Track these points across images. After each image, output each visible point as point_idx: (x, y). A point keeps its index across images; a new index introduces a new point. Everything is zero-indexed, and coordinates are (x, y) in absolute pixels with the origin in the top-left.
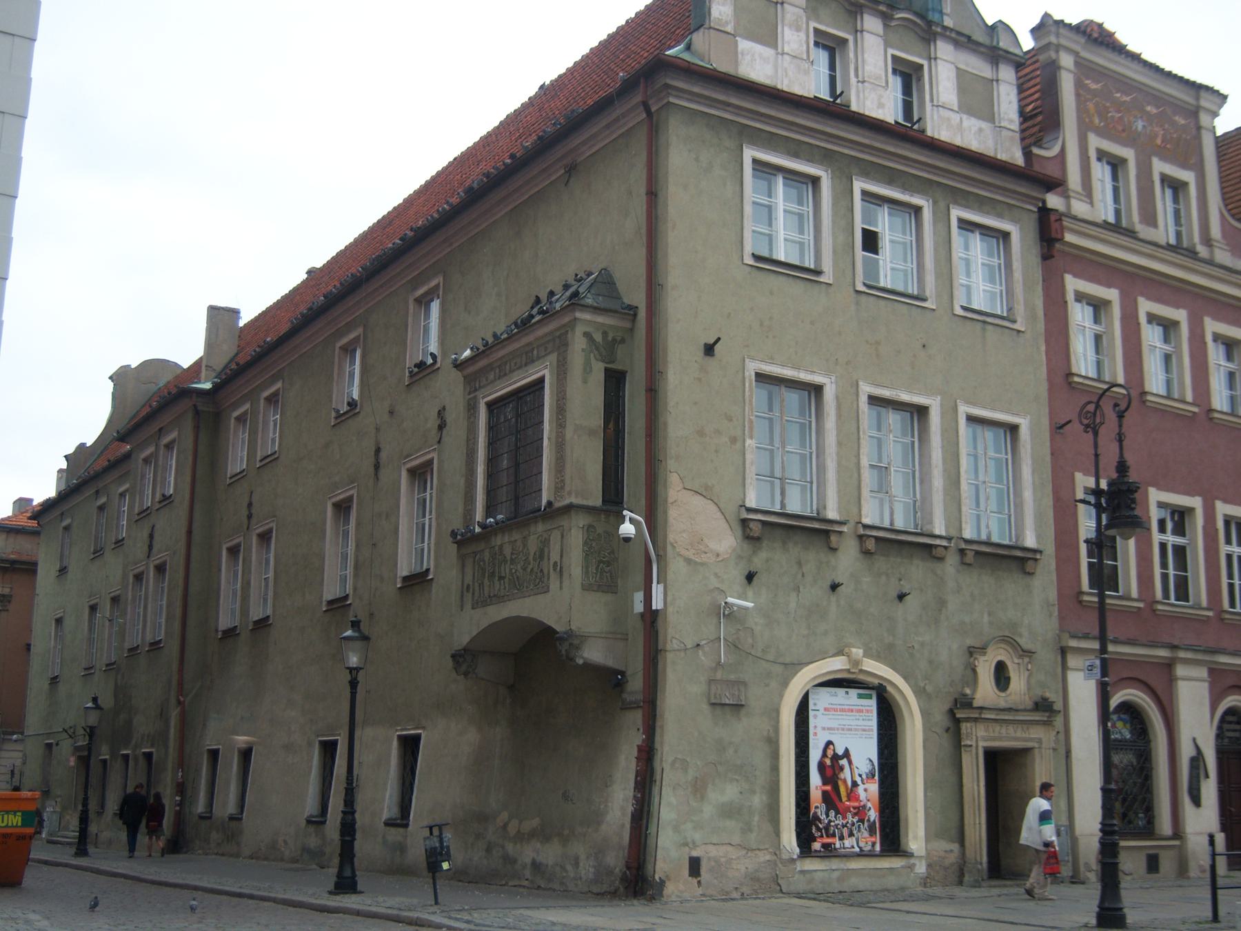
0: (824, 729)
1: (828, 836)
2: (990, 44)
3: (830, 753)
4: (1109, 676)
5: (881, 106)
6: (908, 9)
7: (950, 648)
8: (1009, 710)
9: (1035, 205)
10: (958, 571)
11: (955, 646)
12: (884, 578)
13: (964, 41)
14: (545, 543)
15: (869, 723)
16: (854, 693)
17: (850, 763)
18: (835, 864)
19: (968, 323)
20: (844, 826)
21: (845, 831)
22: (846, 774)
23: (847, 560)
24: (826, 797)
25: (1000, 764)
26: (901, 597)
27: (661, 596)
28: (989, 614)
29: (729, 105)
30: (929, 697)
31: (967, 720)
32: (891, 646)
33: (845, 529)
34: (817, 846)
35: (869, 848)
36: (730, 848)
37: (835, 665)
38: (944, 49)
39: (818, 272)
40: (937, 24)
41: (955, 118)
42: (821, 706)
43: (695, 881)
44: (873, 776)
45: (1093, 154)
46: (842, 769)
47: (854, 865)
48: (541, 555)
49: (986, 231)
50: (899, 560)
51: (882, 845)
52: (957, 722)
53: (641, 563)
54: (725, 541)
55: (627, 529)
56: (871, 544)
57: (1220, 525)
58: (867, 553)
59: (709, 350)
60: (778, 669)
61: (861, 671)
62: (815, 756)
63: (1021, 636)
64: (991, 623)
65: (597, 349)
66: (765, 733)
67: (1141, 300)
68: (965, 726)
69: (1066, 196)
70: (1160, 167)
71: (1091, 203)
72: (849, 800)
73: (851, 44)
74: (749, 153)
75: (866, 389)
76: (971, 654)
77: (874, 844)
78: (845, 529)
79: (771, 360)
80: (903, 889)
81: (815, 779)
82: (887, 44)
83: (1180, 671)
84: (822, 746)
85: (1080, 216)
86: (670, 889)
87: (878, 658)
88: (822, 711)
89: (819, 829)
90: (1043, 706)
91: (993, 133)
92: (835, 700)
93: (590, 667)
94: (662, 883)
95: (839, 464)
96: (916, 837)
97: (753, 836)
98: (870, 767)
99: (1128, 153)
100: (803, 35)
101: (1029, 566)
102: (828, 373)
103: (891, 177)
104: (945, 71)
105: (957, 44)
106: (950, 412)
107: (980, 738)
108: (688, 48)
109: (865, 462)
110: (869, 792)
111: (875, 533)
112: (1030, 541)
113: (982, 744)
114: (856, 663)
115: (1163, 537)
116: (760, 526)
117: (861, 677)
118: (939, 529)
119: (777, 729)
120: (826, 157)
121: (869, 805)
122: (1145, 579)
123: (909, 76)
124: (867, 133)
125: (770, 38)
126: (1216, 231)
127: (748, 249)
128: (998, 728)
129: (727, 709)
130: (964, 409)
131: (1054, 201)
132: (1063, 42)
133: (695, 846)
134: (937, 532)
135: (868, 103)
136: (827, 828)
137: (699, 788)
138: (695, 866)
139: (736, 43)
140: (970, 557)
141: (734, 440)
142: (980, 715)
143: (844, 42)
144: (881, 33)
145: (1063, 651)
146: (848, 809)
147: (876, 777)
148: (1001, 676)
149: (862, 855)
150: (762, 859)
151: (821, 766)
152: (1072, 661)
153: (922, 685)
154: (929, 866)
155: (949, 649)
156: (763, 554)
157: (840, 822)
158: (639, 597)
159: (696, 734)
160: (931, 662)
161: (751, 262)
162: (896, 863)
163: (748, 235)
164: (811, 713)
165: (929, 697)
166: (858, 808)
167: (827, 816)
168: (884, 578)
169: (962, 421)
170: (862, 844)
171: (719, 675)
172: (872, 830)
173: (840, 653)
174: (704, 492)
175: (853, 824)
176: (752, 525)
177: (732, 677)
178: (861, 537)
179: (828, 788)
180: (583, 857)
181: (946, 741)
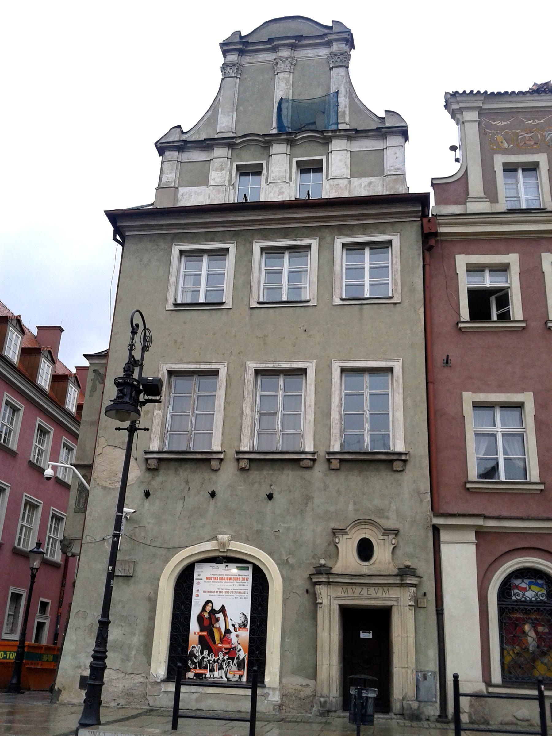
0: (205, 592)
1: (200, 668)
3: (208, 609)
7: (313, 531)
9: (417, 217)
10: (326, 475)
11: (319, 529)
12: (256, 486)
13: (354, 134)
15: (245, 587)
17: (225, 616)
19: (346, 307)
20: (215, 662)
21: (216, 666)
22: (221, 624)
23: (226, 477)
24: (202, 640)
26: (270, 497)
28: (355, 504)
29: (162, 225)
30: (292, 567)
31: (320, 583)
32: (259, 532)
34: (190, 675)
35: (236, 679)
37: (208, 547)
38: (337, 145)
42: (204, 576)
44: (245, 626)
45: (499, 169)
46: (217, 620)
47: (211, 690)
50: (271, 472)
51: (247, 679)
58: (242, 470)
60: (164, 552)
61: (228, 550)
62: (196, 610)
63: (388, 518)
64: (356, 510)
66: (147, 595)
72: (222, 642)
73: (265, 166)
76: (334, 534)
77: (241, 677)
79: (181, 362)
81: (194, 627)
84: (203, 603)
87: (247, 541)
88: (204, 579)
90: (405, 572)
97: (130, 664)
98: (243, 619)
101: (397, 465)
103: (285, 233)
105: (349, 138)
110: (241, 638)
111: (247, 456)
112: (399, 446)
114: (223, 545)
121: (240, 647)
124: (259, 213)
128: (358, 590)
129: (121, 579)
132: (462, 105)
134: (307, 450)
136: (200, 663)
140: (335, 464)
146: (220, 649)
147: (248, 627)
148: (365, 550)
149: (229, 685)
150: (136, 681)
151: (200, 618)
152: (444, 536)
153: (286, 559)
154: (284, 696)
155: (313, 532)
156: (160, 478)
159: (95, 595)
160: (295, 542)
161: (173, 308)
164: (195, 582)
165: (292, 567)
166: (230, 649)
167: (202, 653)
170: (228, 676)
172: (240, 665)
173: (214, 538)
175: (224, 661)
177: (127, 558)
178: (238, 460)
179: (205, 634)
181: (306, 600)
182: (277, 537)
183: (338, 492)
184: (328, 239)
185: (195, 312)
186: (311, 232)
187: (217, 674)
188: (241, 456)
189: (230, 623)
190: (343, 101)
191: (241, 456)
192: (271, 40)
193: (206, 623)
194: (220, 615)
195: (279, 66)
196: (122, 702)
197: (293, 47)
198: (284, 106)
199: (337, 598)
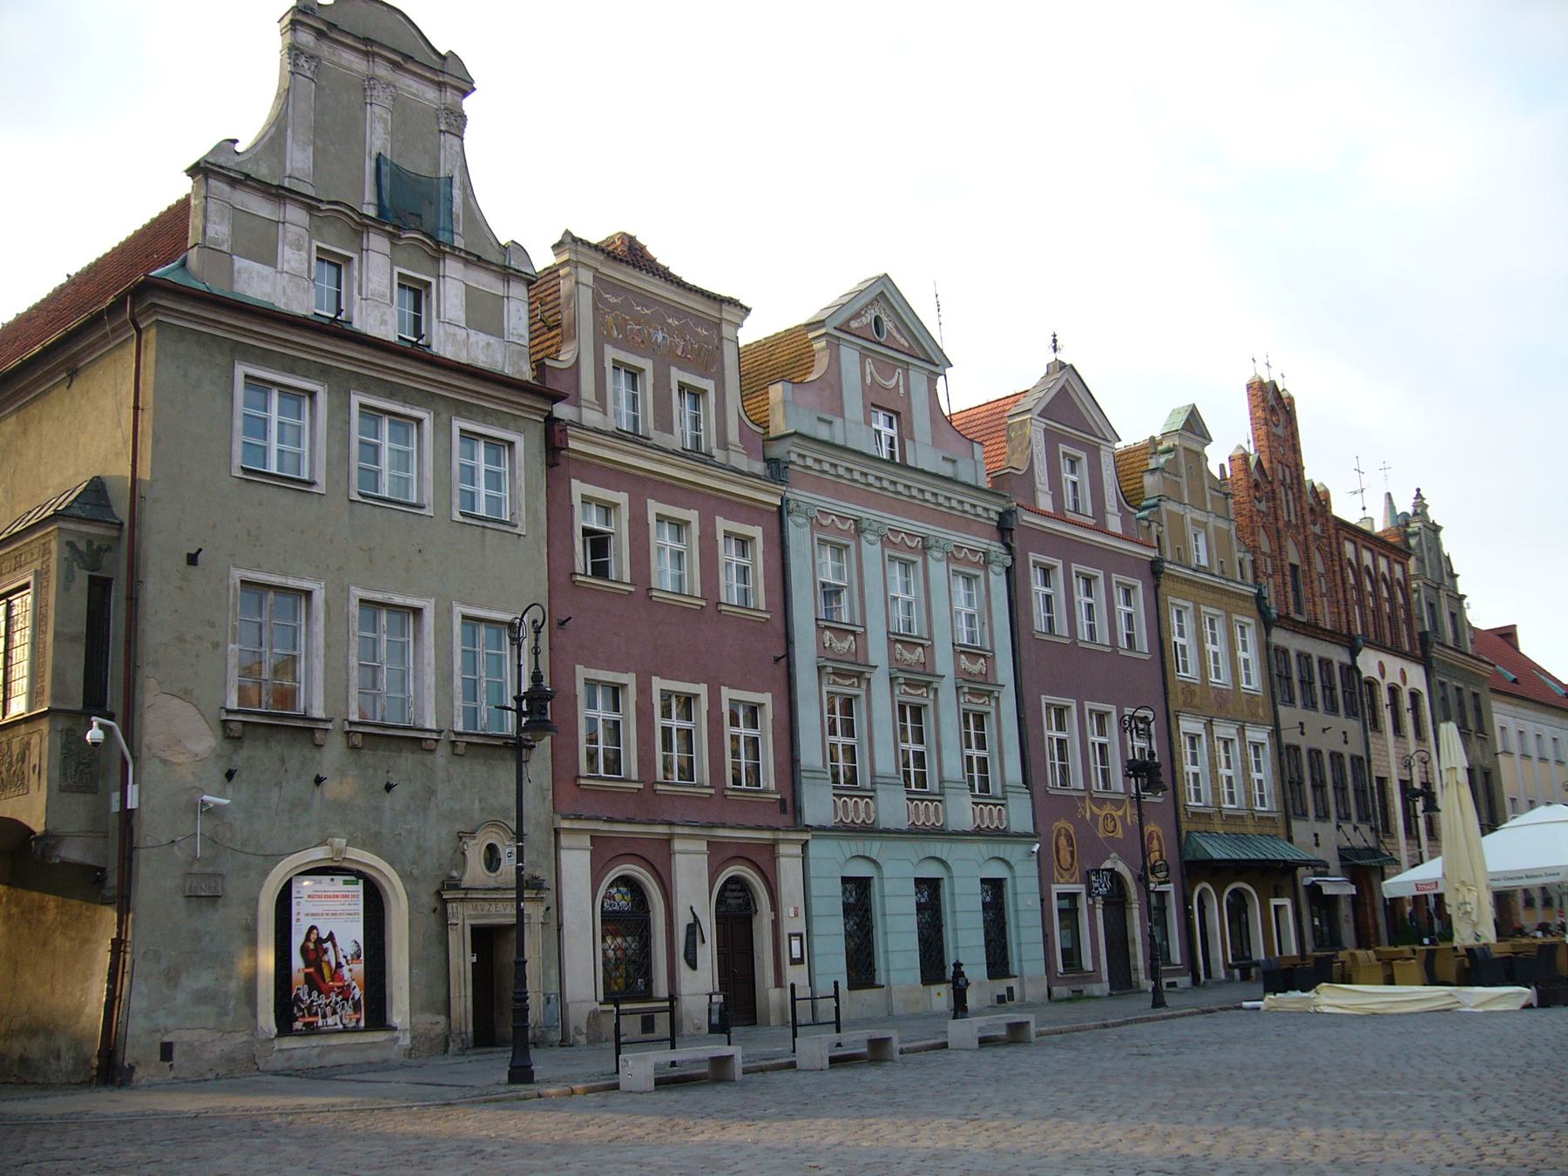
2: (506, 264)
3: (313, 937)
4: (604, 852)
5: (384, 322)
6: (417, 230)
8: (497, 889)
12: (371, 771)
13: (474, 260)
14: (26, 746)
16: (339, 879)
17: (335, 946)
18: (314, 1041)
23: (334, 751)
24: (308, 977)
25: (485, 939)
26: (389, 788)
27: (136, 796)
30: (416, 880)
31: (454, 900)
32: (377, 834)
33: (330, 726)
34: (298, 1025)
36: (203, 1032)
37: (318, 854)
38: (452, 267)
39: (311, 483)
40: (445, 245)
41: (464, 333)
43: (167, 1064)
45: (609, 365)
46: (326, 951)
47: (335, 1040)
48: (22, 759)
49: (491, 441)
52: (445, 901)
53: (119, 763)
54: (205, 742)
55: (94, 734)
56: (357, 740)
57: (726, 709)
58: (354, 748)
59: (192, 559)
62: (297, 940)
65: (81, 557)
67: (651, 502)
68: (449, 906)
69: (577, 404)
70: (677, 375)
71: (605, 413)
74: (241, 370)
75: (358, 593)
77: (358, 1020)
78: (330, 726)
79: (259, 568)
80: (386, 1061)
81: (297, 962)
82: (393, 263)
83: (678, 845)
84: (305, 931)
85: (590, 425)
86: (139, 1073)
87: (363, 847)
89: (300, 1009)
91: (502, 351)
92: (319, 887)
93: (67, 865)
94: (132, 1068)
95: (326, 665)
96: (400, 1011)
99: (646, 364)
100: (304, 254)
102: (317, 579)
103: (392, 391)
104: (453, 288)
105: (466, 262)
106: (444, 613)
107: (464, 917)
108: (184, 264)
109: (354, 662)
110: (354, 973)
111: (361, 729)
113: (468, 922)
114: (340, 852)
115: (667, 722)
116: (240, 726)
117: (346, 864)
118: (430, 723)
119: (255, 920)
120: (323, 373)
122: (646, 762)
123: (417, 292)
125: (269, 257)
126: (733, 435)
127: (238, 461)
130: (459, 610)
131: (562, 411)
133: (167, 1031)
135: (371, 321)
137: (172, 977)
138: (167, 1051)
139: (232, 263)
140: (461, 748)
141: (216, 645)
142: (468, 895)
143: (350, 259)
144: (388, 251)
145: (557, 832)
146: (332, 989)
148: (492, 858)
149: (346, 1030)
152: (565, 840)
154: (413, 1038)
155: (437, 835)
156: (244, 753)
157: (323, 1001)
158: (116, 796)
160: (419, 848)
162: (380, 1036)
163: (238, 450)
164: (294, 901)
165: (416, 880)
168: (371, 771)
169: (457, 621)
171: (196, 868)
173: (323, 843)
174: (186, 695)
176: (232, 725)
177: (209, 870)
178: (347, 733)
180: (63, 1051)
181: (433, 922)
182: (398, 842)
183: (463, 784)
184: (444, 417)
185: (275, 490)
186: (425, 399)
187: (330, 1021)
188: (354, 729)
189: (341, 954)
190: (457, 193)
191: (354, 729)
192: (367, 41)
193: (312, 956)
194: (328, 945)
195: (375, 93)
196: (222, 1071)
197: (396, 65)
198: (385, 169)
199: (471, 917)
